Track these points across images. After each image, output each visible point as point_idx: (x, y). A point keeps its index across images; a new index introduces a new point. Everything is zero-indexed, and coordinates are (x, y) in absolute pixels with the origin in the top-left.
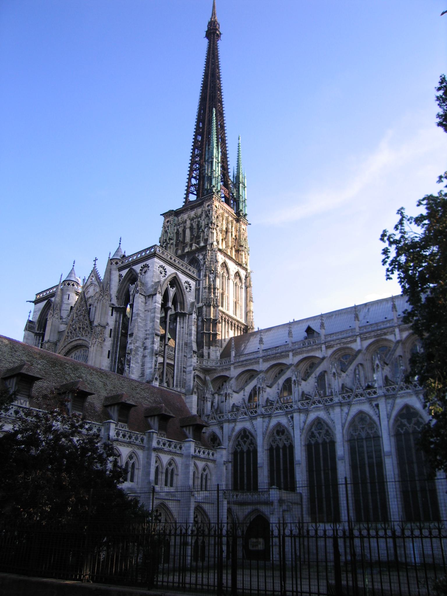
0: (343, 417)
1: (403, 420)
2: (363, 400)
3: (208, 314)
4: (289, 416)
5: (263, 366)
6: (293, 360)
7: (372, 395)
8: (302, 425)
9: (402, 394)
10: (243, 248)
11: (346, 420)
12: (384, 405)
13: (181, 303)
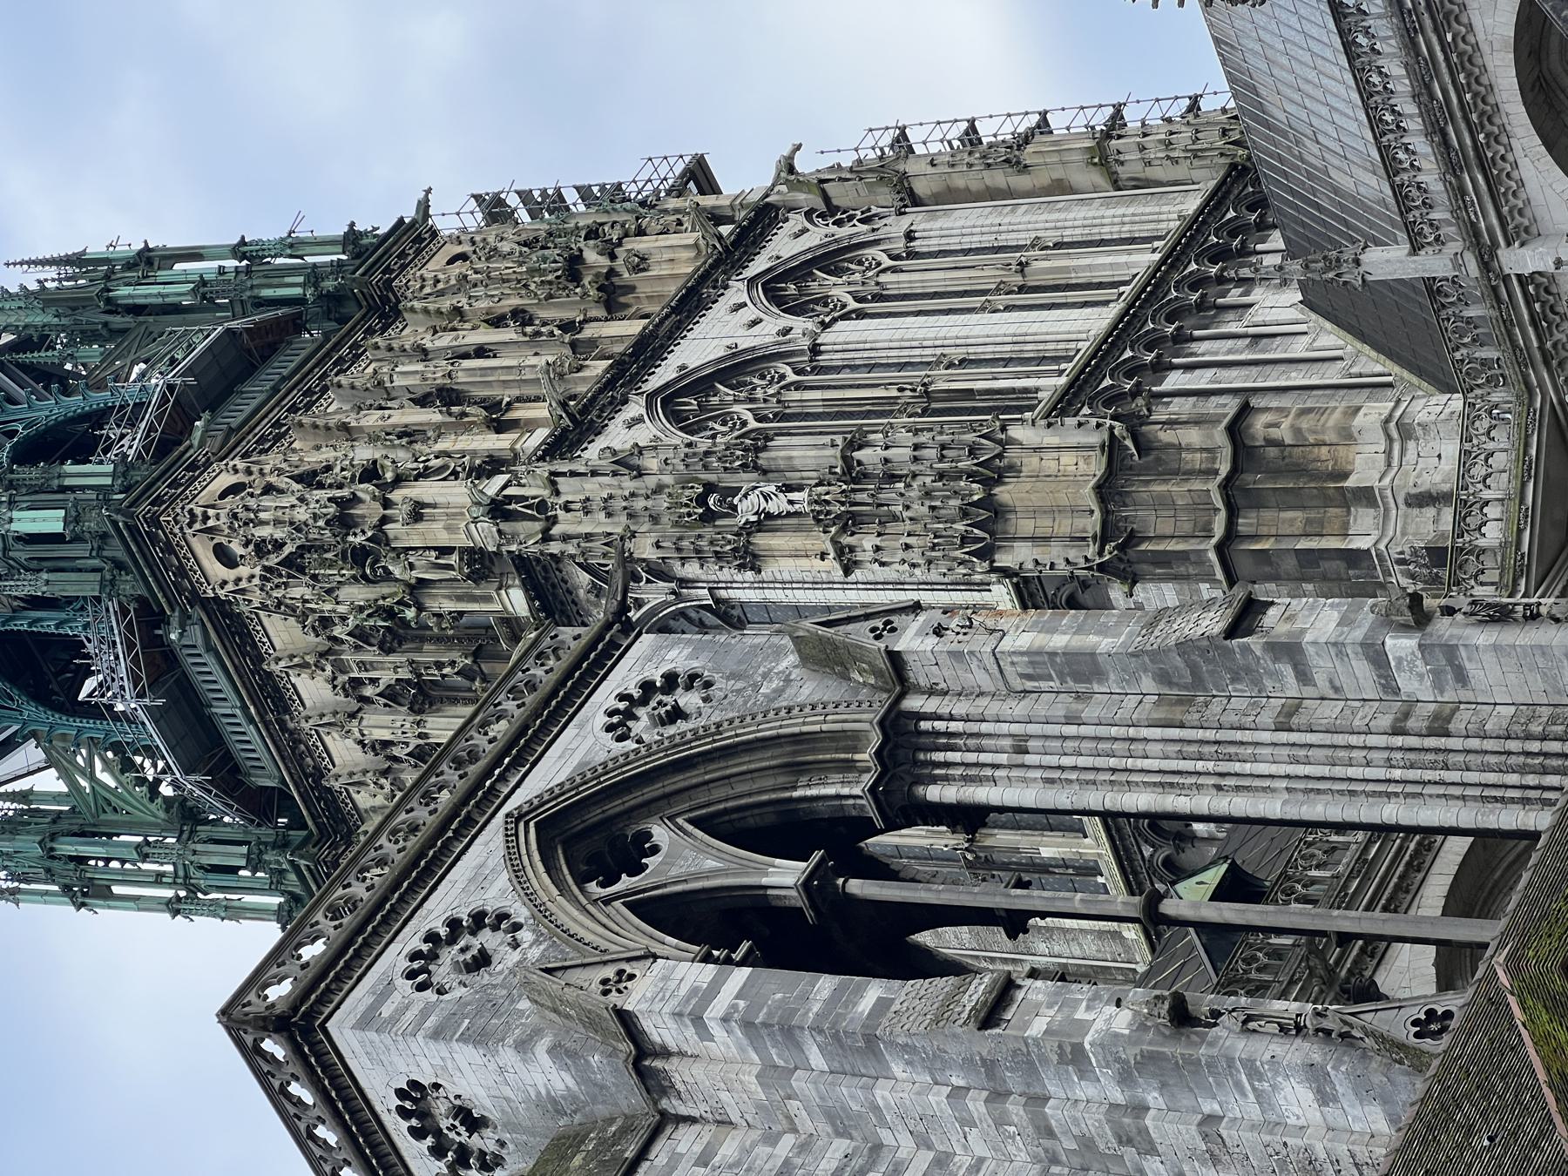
3: (1065, 526)
10: (591, 256)
13: (797, 769)
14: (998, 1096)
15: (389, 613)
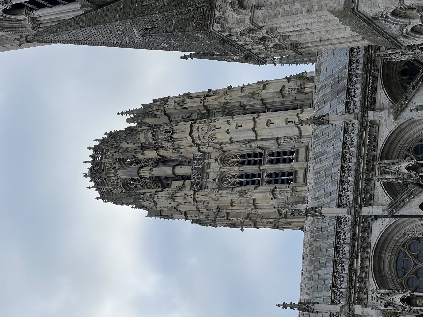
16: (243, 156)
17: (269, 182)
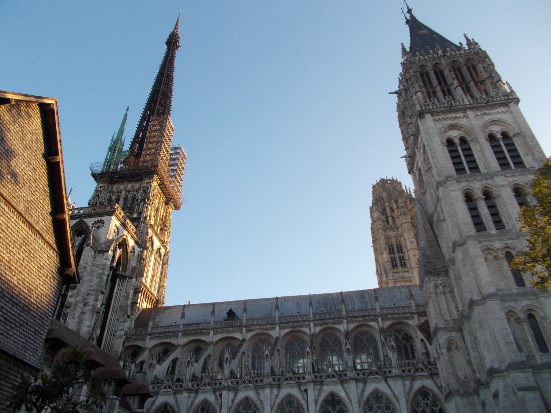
0: (273, 398)
1: (328, 407)
2: (293, 384)
4: (217, 394)
5: (182, 340)
6: (213, 338)
7: (301, 380)
8: (230, 403)
9: (329, 382)
11: (275, 401)
12: (312, 391)
14: (93, 290)
15: (137, 200)
16: (400, 245)
17: (391, 258)
